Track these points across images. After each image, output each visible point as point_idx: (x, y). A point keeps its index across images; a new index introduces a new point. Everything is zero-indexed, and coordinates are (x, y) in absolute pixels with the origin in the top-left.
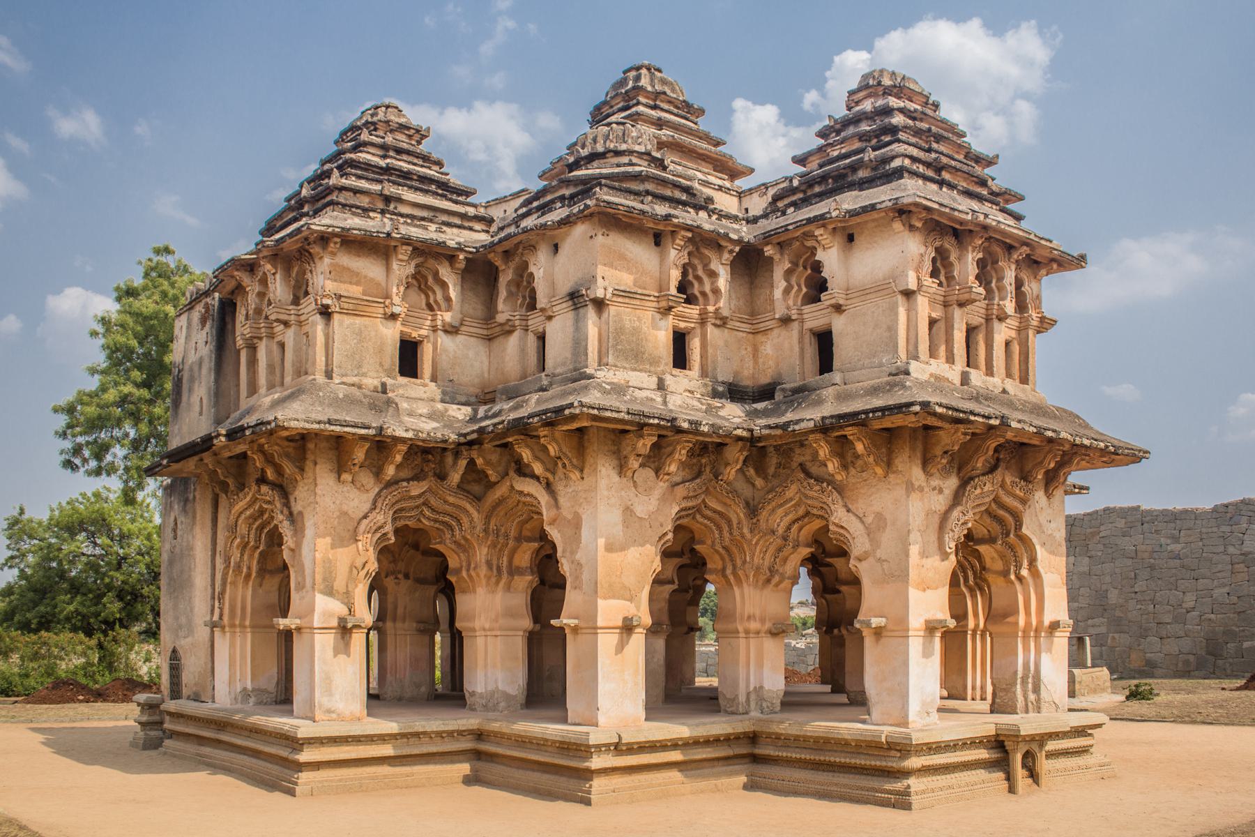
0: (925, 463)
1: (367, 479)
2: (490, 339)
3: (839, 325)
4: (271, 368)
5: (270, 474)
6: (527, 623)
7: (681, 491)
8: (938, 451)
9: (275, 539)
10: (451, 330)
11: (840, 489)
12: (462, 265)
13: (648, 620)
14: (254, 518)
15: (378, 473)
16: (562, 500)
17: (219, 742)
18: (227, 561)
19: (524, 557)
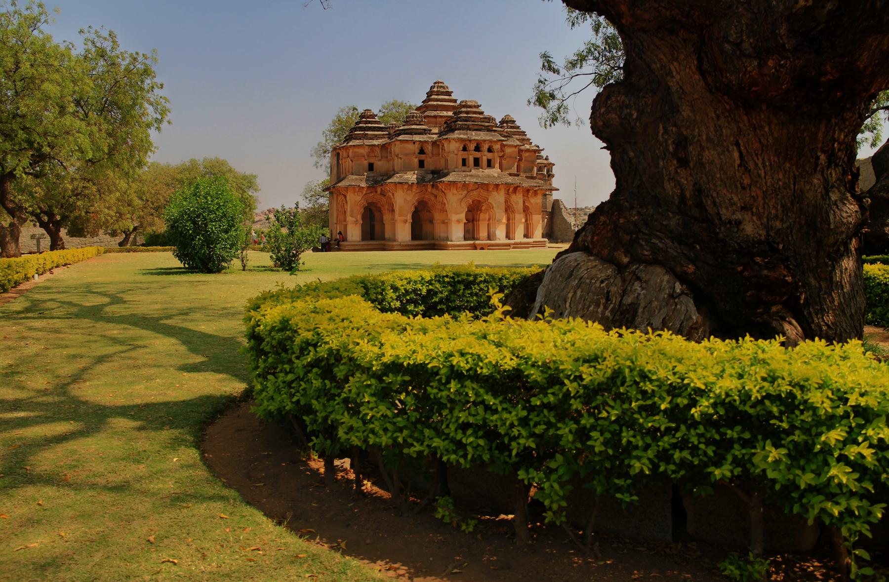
10: (380, 160)
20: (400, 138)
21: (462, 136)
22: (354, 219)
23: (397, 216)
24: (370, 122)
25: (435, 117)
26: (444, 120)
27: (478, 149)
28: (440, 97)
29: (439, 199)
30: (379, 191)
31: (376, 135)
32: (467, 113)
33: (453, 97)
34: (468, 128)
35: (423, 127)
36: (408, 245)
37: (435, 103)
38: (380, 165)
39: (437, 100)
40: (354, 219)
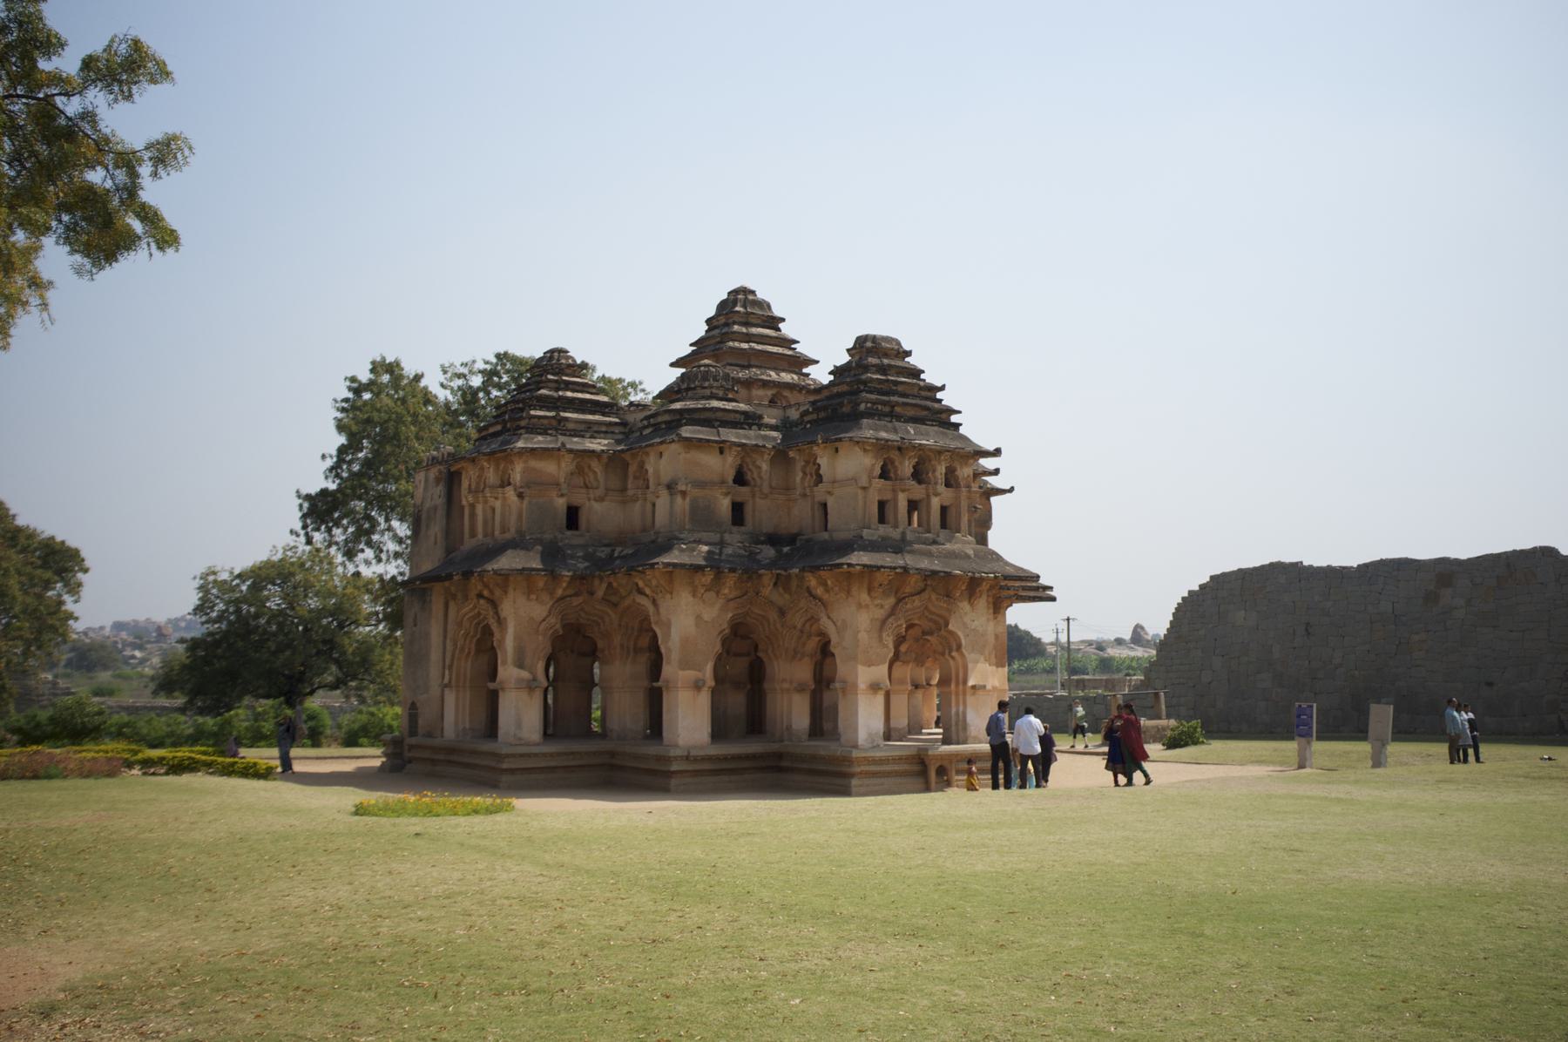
0: (870, 590)
1: (545, 597)
2: (624, 502)
3: (831, 502)
4: (485, 522)
5: (486, 593)
6: (646, 683)
7: (732, 604)
8: (876, 584)
9: (487, 632)
10: (601, 499)
11: (824, 605)
12: (605, 460)
13: (711, 682)
14: (474, 617)
15: (552, 594)
16: (662, 610)
17: (450, 762)
18: (455, 645)
19: (645, 641)
20: (687, 431)
21: (884, 435)
22: (525, 674)
23: (668, 670)
24: (568, 386)
25: (749, 384)
26: (770, 393)
27: (918, 475)
28: (754, 330)
29: (798, 620)
30: (600, 593)
31: (589, 423)
32: (883, 370)
33: (786, 329)
34: (892, 415)
35: (742, 406)
36: (709, 759)
37: (745, 346)
38: (602, 513)
39: (748, 338)
40: (525, 674)
